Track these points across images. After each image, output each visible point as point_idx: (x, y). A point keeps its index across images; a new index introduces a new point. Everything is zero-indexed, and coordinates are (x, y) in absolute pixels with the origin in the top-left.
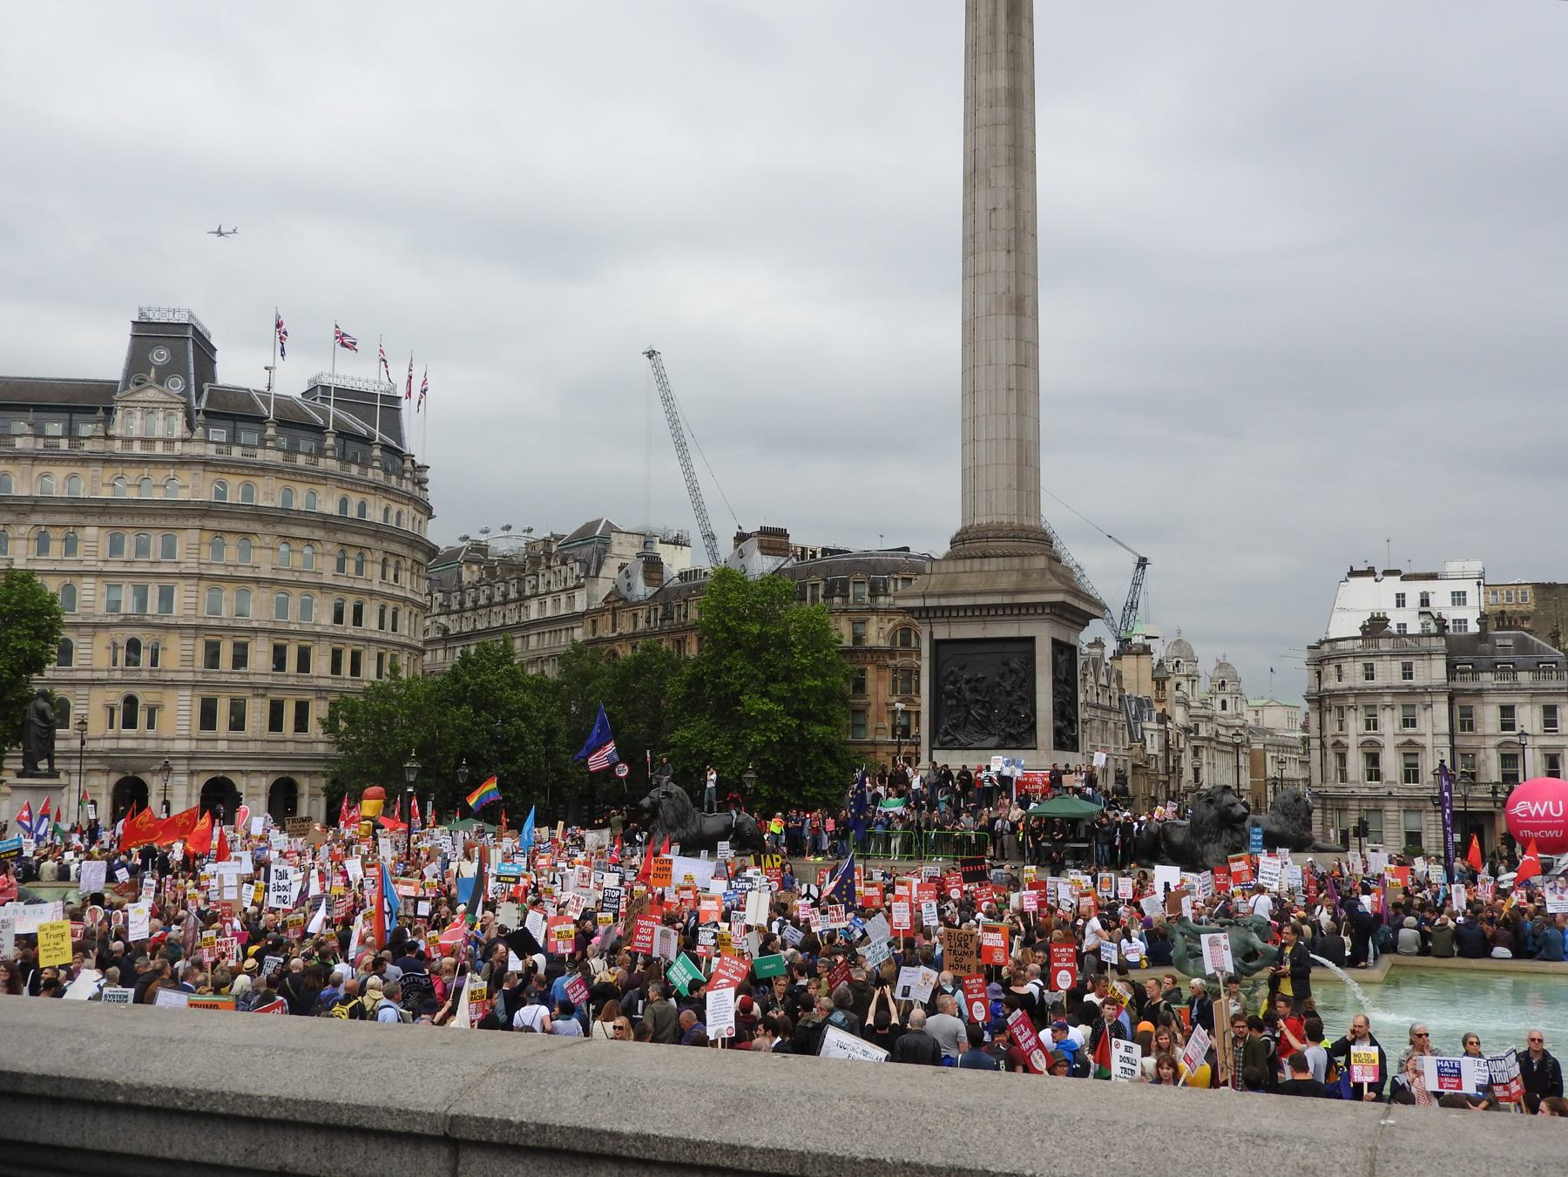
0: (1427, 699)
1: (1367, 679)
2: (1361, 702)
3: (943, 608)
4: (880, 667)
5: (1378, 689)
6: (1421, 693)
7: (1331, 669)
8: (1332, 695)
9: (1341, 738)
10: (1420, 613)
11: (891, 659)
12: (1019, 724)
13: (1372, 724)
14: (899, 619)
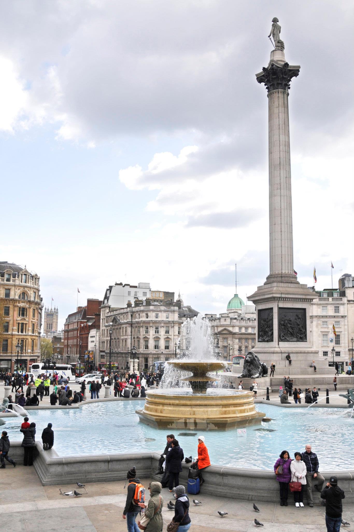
0: (173, 325)
1: (156, 318)
2: (154, 325)
3: (284, 298)
4: (14, 306)
5: (160, 321)
6: (171, 323)
7: (144, 314)
8: (144, 322)
9: (147, 336)
10: (135, 298)
11: (18, 303)
12: (302, 334)
13: (157, 332)
14: (22, 289)
